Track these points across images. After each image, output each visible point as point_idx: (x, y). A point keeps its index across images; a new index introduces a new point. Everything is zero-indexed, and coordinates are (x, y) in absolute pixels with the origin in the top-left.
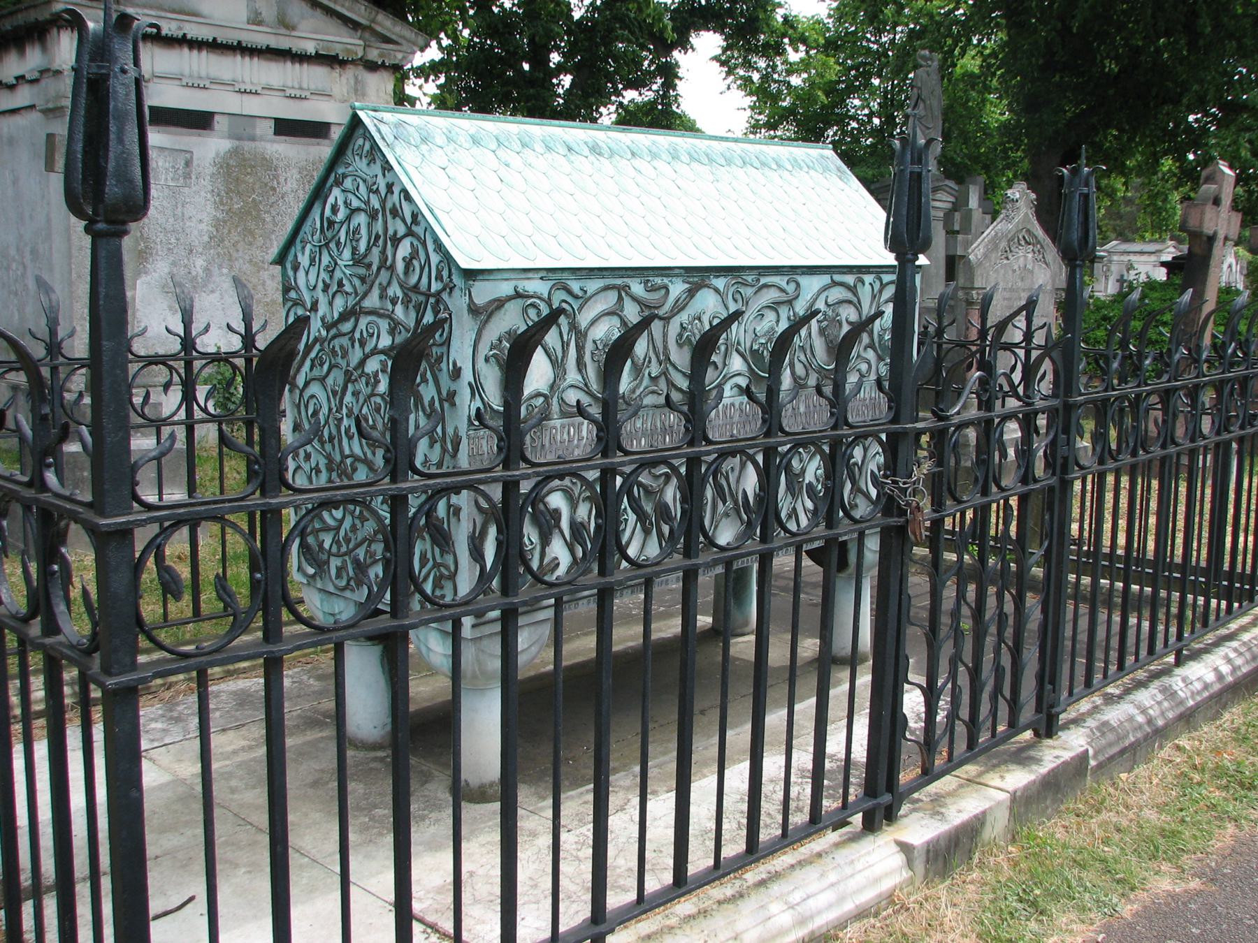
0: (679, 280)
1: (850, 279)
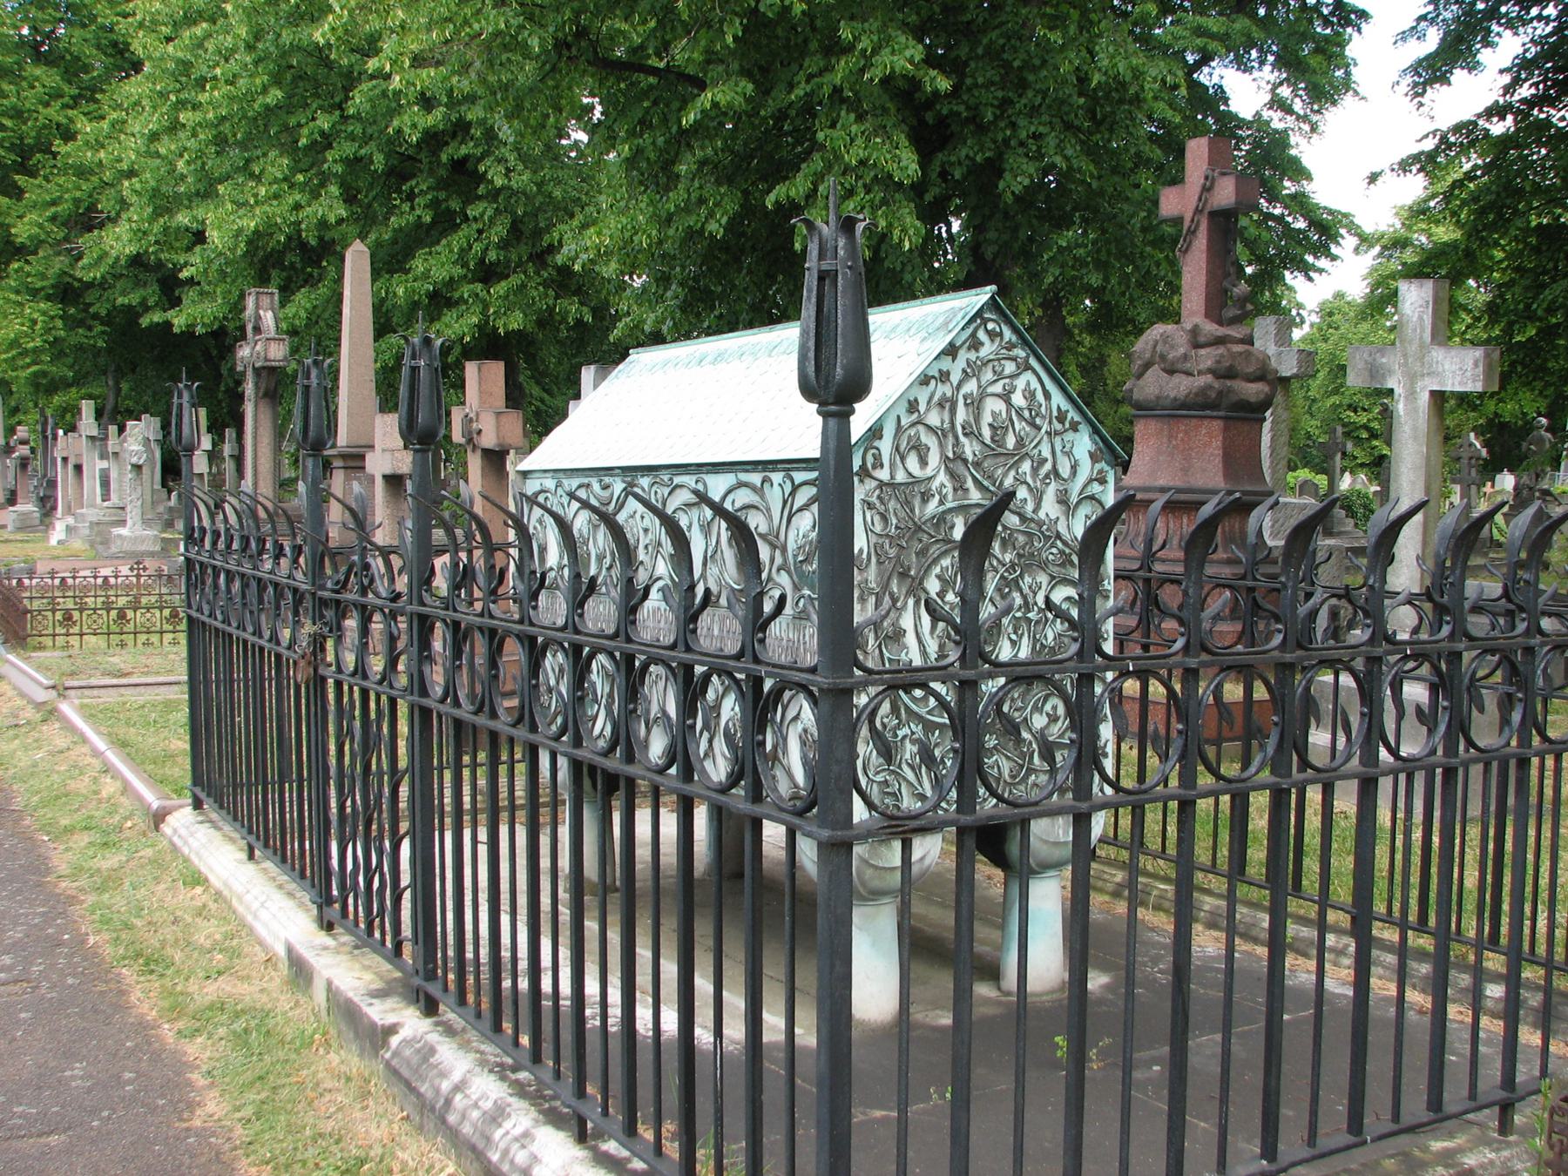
0: (618, 479)
1: (755, 478)
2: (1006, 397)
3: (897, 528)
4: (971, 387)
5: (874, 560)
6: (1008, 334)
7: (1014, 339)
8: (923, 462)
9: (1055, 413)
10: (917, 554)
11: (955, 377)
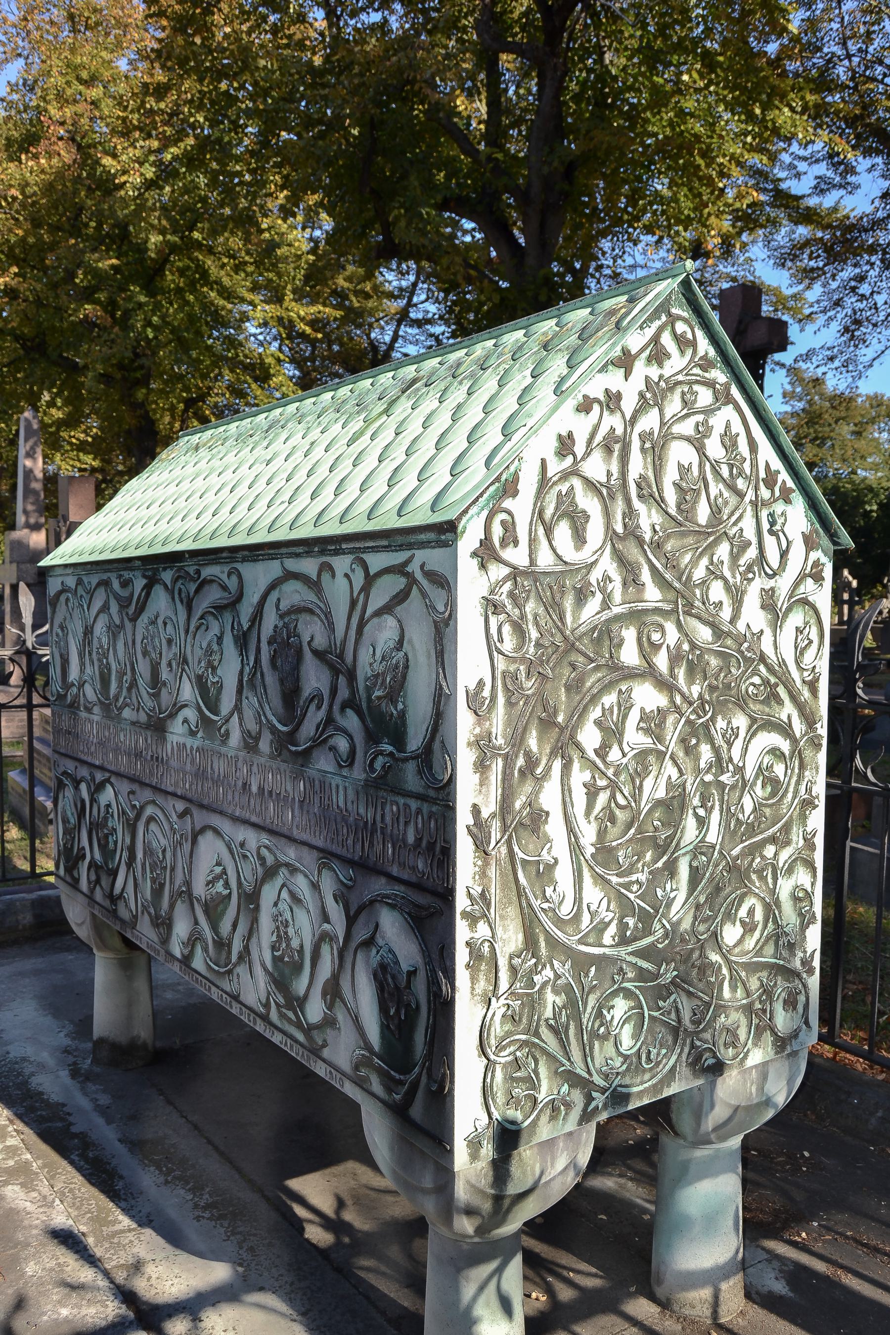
0: (138, 573)
1: (309, 566)
2: (698, 443)
3: (538, 645)
4: (650, 421)
5: (501, 700)
6: (704, 346)
7: (712, 352)
8: (580, 538)
9: (762, 475)
10: (568, 688)
11: (629, 404)
